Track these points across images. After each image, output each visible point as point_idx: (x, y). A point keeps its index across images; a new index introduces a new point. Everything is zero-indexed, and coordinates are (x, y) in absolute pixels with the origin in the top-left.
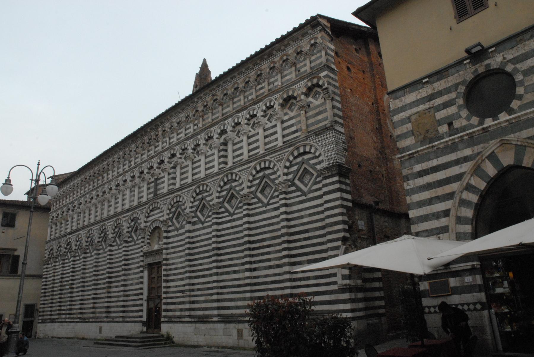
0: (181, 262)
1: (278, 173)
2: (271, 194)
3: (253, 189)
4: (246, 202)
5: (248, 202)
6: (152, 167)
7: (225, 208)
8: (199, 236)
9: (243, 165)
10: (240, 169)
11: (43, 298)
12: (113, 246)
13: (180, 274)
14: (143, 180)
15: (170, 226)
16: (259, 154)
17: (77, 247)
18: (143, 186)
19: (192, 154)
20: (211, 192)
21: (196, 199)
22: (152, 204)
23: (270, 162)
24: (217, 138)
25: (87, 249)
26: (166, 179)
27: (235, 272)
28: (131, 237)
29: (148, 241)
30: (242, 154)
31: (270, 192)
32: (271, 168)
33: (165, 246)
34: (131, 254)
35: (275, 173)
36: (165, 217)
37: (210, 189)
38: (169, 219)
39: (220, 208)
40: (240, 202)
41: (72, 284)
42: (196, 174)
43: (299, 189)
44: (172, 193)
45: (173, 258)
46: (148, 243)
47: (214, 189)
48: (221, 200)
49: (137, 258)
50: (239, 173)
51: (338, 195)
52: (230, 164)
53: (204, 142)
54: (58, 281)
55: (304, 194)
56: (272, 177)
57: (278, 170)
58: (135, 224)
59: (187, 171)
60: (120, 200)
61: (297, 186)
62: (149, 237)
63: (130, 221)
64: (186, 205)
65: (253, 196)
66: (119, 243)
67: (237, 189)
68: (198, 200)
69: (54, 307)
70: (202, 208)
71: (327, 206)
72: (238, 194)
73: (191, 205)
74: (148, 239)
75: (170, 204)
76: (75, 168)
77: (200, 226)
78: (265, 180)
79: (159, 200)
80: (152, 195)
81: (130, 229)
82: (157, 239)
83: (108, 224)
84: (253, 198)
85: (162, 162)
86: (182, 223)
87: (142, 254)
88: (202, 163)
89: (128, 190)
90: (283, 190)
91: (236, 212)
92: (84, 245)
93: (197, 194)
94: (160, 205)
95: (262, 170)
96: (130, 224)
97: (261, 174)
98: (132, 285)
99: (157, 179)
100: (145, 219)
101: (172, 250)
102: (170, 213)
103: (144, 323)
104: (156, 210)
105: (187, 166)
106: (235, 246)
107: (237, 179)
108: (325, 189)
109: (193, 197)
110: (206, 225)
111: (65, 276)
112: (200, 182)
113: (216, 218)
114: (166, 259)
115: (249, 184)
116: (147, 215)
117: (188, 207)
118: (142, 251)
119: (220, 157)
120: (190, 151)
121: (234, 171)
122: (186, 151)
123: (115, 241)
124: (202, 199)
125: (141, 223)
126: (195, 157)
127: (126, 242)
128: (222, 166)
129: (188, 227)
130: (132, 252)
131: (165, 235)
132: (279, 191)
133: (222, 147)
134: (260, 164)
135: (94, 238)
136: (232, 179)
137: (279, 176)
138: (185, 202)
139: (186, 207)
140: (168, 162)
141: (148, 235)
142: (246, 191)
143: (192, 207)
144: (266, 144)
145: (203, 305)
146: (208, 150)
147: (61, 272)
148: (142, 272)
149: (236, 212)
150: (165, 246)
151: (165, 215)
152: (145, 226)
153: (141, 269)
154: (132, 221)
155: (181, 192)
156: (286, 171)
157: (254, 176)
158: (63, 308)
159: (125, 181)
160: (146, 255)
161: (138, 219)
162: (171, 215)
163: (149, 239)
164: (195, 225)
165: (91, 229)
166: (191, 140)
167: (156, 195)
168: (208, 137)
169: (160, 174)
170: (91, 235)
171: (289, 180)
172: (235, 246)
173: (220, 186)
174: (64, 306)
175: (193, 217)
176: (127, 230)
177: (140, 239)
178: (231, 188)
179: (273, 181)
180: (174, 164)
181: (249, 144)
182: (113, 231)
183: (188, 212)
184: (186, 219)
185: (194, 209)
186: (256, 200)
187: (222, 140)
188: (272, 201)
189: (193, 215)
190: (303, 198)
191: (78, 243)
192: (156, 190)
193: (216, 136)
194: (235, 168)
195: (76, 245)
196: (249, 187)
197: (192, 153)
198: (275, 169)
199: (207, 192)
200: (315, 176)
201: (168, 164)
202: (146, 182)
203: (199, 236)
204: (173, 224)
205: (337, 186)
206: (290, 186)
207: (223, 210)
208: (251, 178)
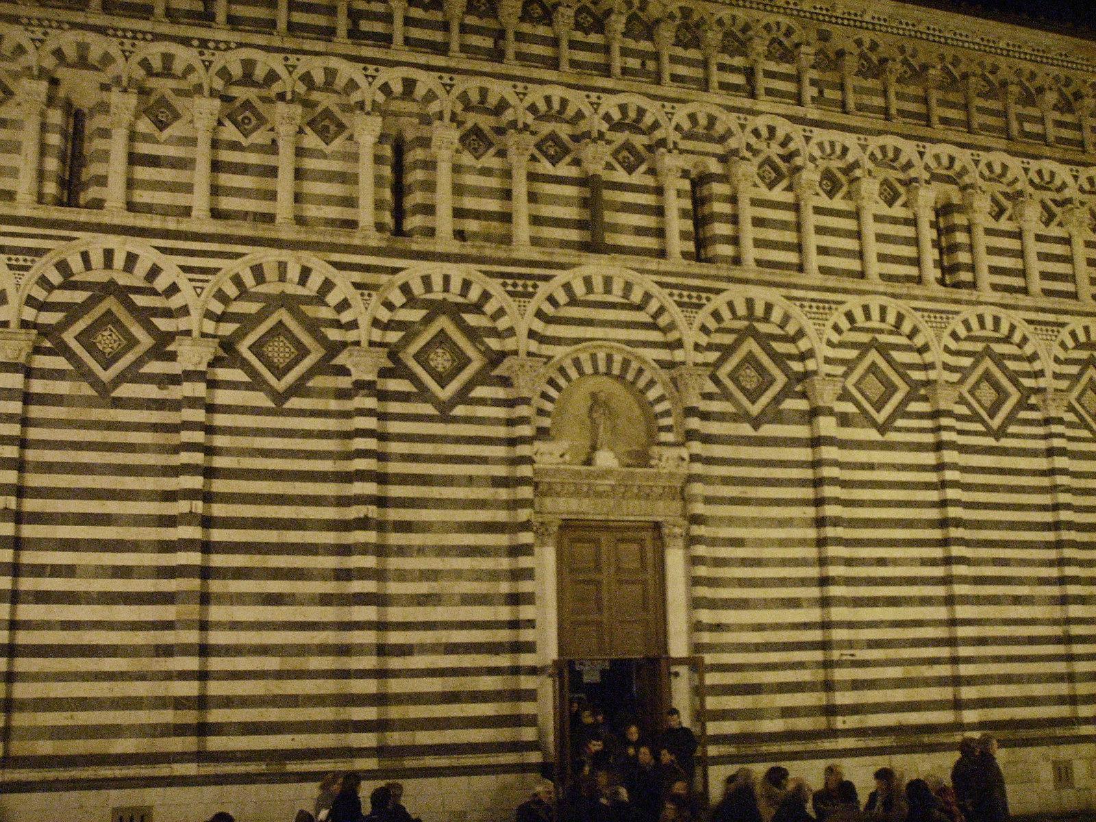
0: (783, 543)
8: (871, 467)
10: (1033, 316)
13: (782, 582)
15: (708, 396)
27: (1017, 600)
29: (546, 422)
33: (698, 468)
45: (731, 521)
49: (470, 481)
58: (427, 321)
63: (398, 298)
68: (854, 345)
70: (888, 379)
74: (541, 412)
75: (716, 315)
87: (525, 471)
100: (538, 326)
102: (710, 347)
106: (1013, 526)
110: (893, 436)
118: (528, 460)
121: (1012, 312)
124: (864, 348)
145: (899, 695)
148: (526, 550)
150: (698, 468)
153: (526, 538)
154: (412, 301)
155: (783, 291)
162: (712, 356)
166: (816, 130)
172: (1013, 526)
177: (482, 402)
203: (871, 467)
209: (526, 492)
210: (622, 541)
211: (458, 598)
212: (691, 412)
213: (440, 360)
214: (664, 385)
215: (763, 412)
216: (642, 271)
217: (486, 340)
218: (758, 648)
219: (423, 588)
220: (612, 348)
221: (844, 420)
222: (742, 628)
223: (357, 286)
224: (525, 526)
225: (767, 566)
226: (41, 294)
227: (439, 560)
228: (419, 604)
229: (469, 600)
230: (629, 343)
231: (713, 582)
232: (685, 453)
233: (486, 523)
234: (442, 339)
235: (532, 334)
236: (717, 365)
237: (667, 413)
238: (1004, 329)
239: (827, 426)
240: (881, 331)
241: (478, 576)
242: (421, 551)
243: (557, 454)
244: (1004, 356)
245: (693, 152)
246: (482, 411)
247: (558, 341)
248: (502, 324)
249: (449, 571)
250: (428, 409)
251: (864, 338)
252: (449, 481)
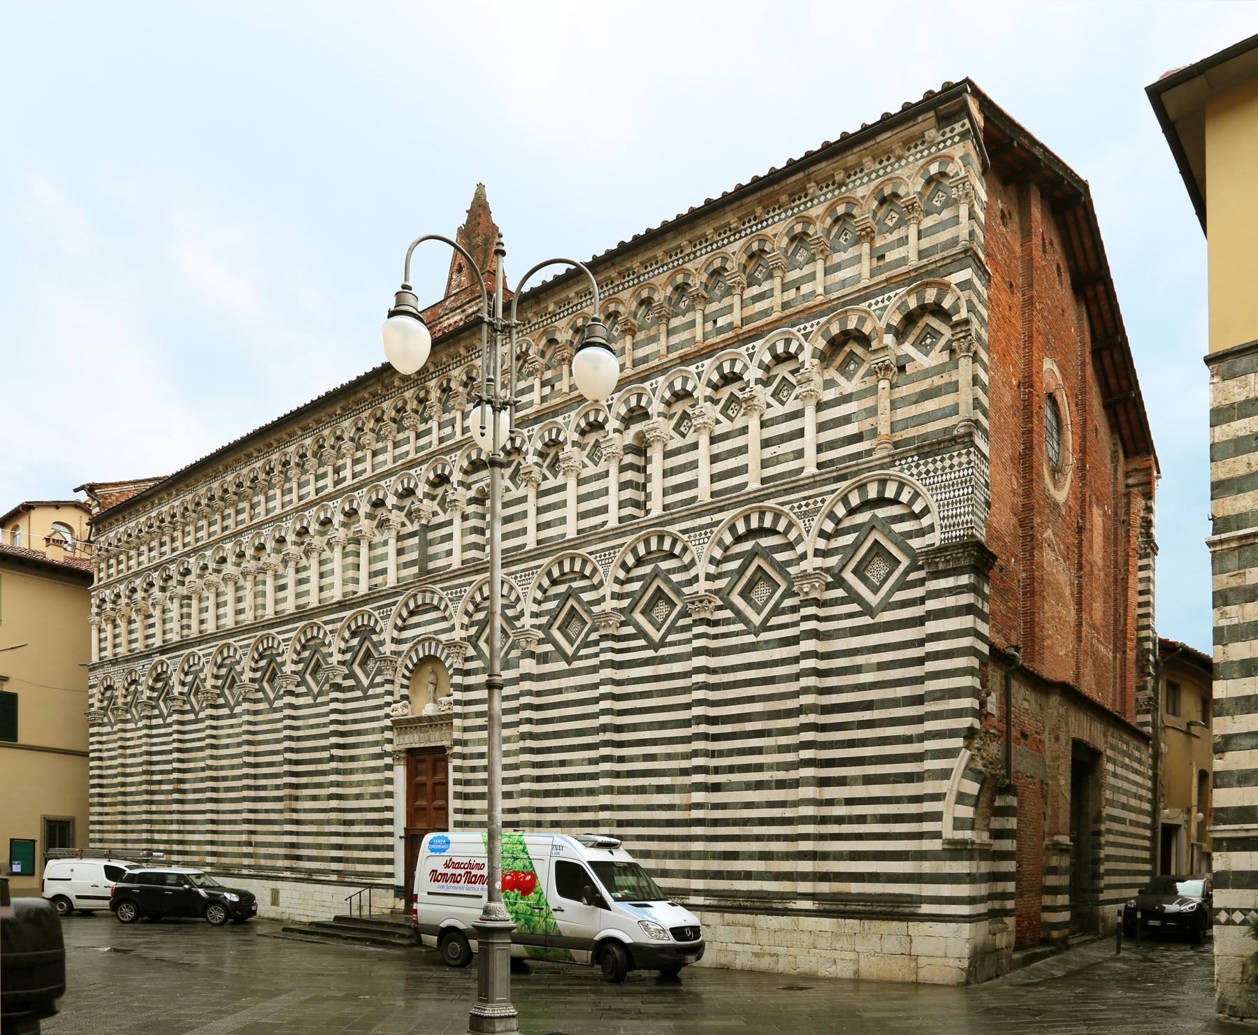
1: (800, 549)
2: (772, 602)
3: (722, 583)
4: (703, 615)
5: (708, 616)
6: (409, 492)
7: (636, 625)
9: (700, 515)
11: (98, 809)
12: (298, 695)
14: (383, 524)
16: (748, 489)
17: (186, 689)
18: (385, 543)
19: (536, 469)
20: (596, 580)
21: (548, 594)
22: (415, 596)
23: (777, 516)
24: (616, 431)
25: (219, 696)
26: (456, 528)
28: (352, 675)
29: (405, 692)
30: (693, 484)
31: (770, 597)
32: (778, 533)
35: (790, 546)
36: (458, 634)
37: (595, 570)
38: (469, 639)
39: (623, 624)
40: (684, 614)
41: (180, 781)
42: (548, 525)
43: (853, 597)
44: (477, 572)
46: (404, 697)
47: (606, 573)
48: (625, 603)
50: (685, 537)
51: (967, 621)
52: (656, 509)
53: (576, 437)
54: (139, 769)
55: (868, 610)
56: (780, 557)
57: (800, 539)
58: (361, 644)
59: (524, 514)
60: (313, 573)
61: (849, 589)
62: (405, 682)
63: (347, 635)
64: (519, 607)
65: (720, 602)
66: (316, 689)
67: (675, 578)
68: (556, 596)
69: (132, 832)
71: (931, 647)
72: (679, 594)
73: (535, 608)
74: (402, 686)
76: (169, 467)
77: (563, 665)
78: (758, 561)
79: (437, 587)
80: (415, 570)
81: (348, 656)
82: (431, 687)
83: (281, 637)
84: (719, 608)
85: (443, 480)
86: (507, 653)
88: (571, 493)
89: (338, 549)
90: (812, 596)
91: (670, 638)
92: (208, 685)
93: (554, 582)
94: (441, 599)
95: (751, 534)
96: (347, 641)
97: (747, 546)
99: (427, 528)
100: (395, 634)
102: (472, 624)
104: (426, 611)
105: (523, 499)
107: (677, 551)
108: (932, 605)
109: (540, 587)
111: (155, 758)
112: (563, 549)
113: (613, 650)
115: (712, 569)
116: (399, 622)
117: (527, 614)
119: (623, 486)
120: (532, 459)
122: (516, 458)
123: (303, 682)
125: (382, 643)
126: (545, 478)
127: (337, 687)
128: (629, 510)
129: (528, 666)
131: (457, 679)
132: (802, 598)
133: (629, 459)
134: (747, 519)
135: (238, 668)
136: (660, 550)
137: (803, 556)
138: (518, 599)
139: (522, 614)
140: (461, 483)
142: (702, 586)
143: (535, 615)
144: (765, 464)
146: (587, 461)
147: (144, 748)
149: (670, 638)
151: (458, 627)
152: (394, 653)
154: (354, 634)
156: (822, 544)
157: (726, 549)
158: (157, 836)
159: (327, 522)
161: (373, 631)
163: (407, 687)
164: (546, 662)
165: (228, 646)
167: (425, 571)
168: (589, 424)
169: (435, 514)
170: (228, 662)
171: (828, 570)
173: (624, 565)
174: (159, 832)
175: (540, 642)
176: (338, 657)
177: (378, 685)
178: (656, 574)
179: (782, 567)
180: (481, 491)
181: (714, 459)
182: (295, 657)
183: (527, 627)
184: (523, 644)
185: (544, 620)
186: (728, 614)
187: (629, 438)
188: (774, 621)
189: (542, 635)
190: (866, 620)
191: (189, 679)
192: (425, 558)
193: (613, 424)
194: (672, 522)
195: (183, 684)
196: (709, 577)
197: (536, 464)
198: (792, 536)
199: (584, 577)
200: (902, 568)
201: (460, 489)
202: (394, 533)
205: (966, 599)
206: (829, 587)
207: (630, 630)
208: (718, 554)
216: (434, 583)
221: (543, 658)
223: (331, 632)
226: (253, 665)
230: (436, 633)
234: (368, 655)
238: (667, 545)
239: (528, 666)
240: (574, 580)
244: (669, 571)
245: (476, 482)
251: (562, 588)
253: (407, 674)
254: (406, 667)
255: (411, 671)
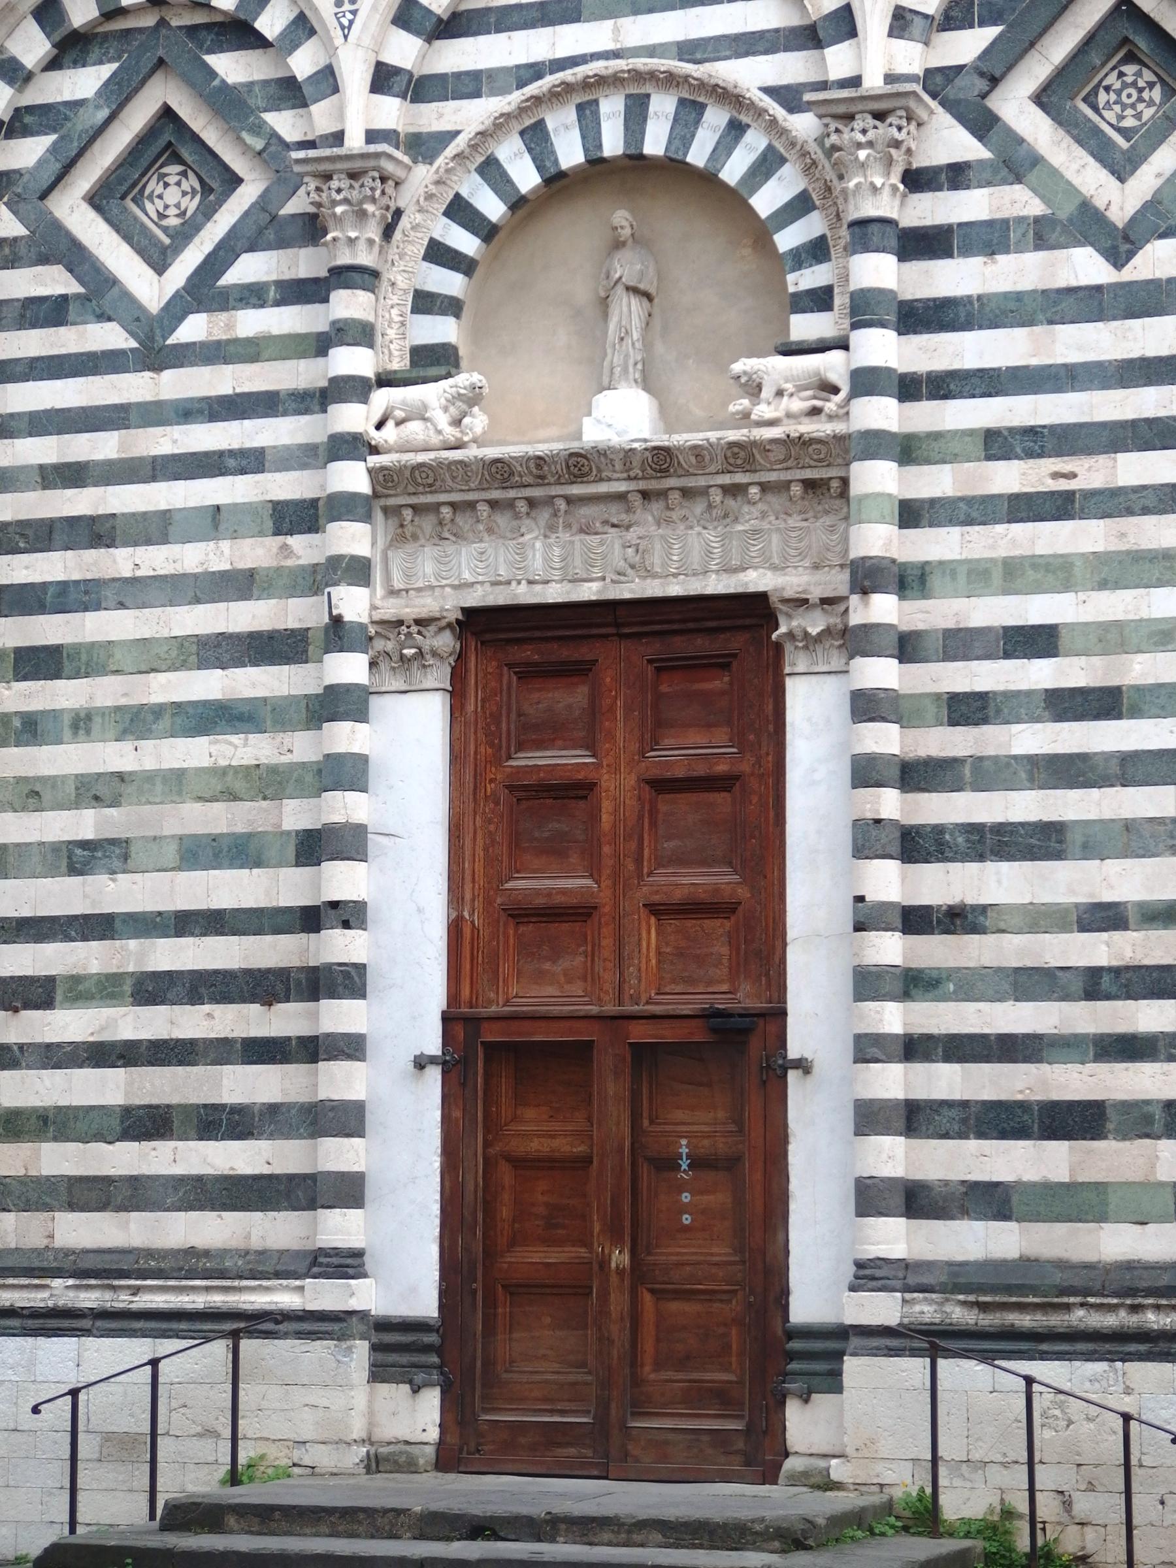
15: (956, 176)
29: (440, 330)
33: (881, 413)
34: (72, 475)
38: (938, 81)
49: (214, 522)
58: (119, 94)
74: (425, 302)
98: (79, 858)
100: (404, 51)
101: (1009, 477)
103: (397, 1349)
114: (909, 580)
118: (350, 446)
130: (103, 446)
141: (438, 253)
150: (881, 413)
154: (71, 48)
160: (418, 497)
163: (452, 307)
204: (1015, 163)
209: (352, 538)
210: (663, 668)
211: (170, 853)
212: (866, 233)
213: (172, 195)
214: (810, 168)
215: (1152, 206)
217: (270, 118)
218: (1094, 984)
219: (84, 824)
220: (638, 76)
222: (1043, 918)
224: (339, 634)
225: (1136, 713)
227: (127, 746)
228: (74, 870)
229: (202, 853)
230: (690, 50)
231: (915, 775)
232: (833, 365)
233: (252, 636)
234: (167, 140)
235: (384, 79)
236: (993, 71)
237: (817, 250)
241: (228, 785)
242: (82, 724)
243: (442, 420)
246: (251, 322)
247: (469, 85)
248: (303, 63)
249: (150, 777)
250: (110, 336)
252: (156, 528)
253: (466, 242)
254: (460, 211)
255: (487, 231)
